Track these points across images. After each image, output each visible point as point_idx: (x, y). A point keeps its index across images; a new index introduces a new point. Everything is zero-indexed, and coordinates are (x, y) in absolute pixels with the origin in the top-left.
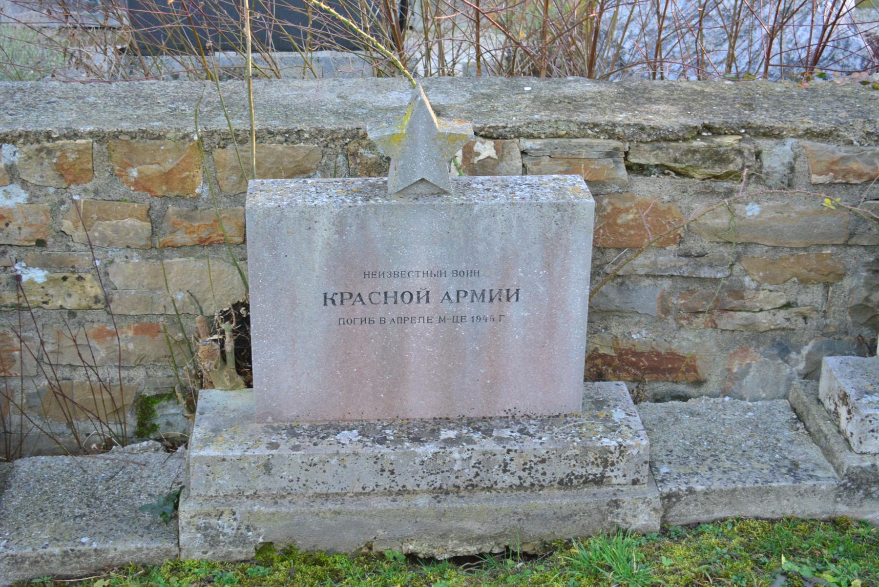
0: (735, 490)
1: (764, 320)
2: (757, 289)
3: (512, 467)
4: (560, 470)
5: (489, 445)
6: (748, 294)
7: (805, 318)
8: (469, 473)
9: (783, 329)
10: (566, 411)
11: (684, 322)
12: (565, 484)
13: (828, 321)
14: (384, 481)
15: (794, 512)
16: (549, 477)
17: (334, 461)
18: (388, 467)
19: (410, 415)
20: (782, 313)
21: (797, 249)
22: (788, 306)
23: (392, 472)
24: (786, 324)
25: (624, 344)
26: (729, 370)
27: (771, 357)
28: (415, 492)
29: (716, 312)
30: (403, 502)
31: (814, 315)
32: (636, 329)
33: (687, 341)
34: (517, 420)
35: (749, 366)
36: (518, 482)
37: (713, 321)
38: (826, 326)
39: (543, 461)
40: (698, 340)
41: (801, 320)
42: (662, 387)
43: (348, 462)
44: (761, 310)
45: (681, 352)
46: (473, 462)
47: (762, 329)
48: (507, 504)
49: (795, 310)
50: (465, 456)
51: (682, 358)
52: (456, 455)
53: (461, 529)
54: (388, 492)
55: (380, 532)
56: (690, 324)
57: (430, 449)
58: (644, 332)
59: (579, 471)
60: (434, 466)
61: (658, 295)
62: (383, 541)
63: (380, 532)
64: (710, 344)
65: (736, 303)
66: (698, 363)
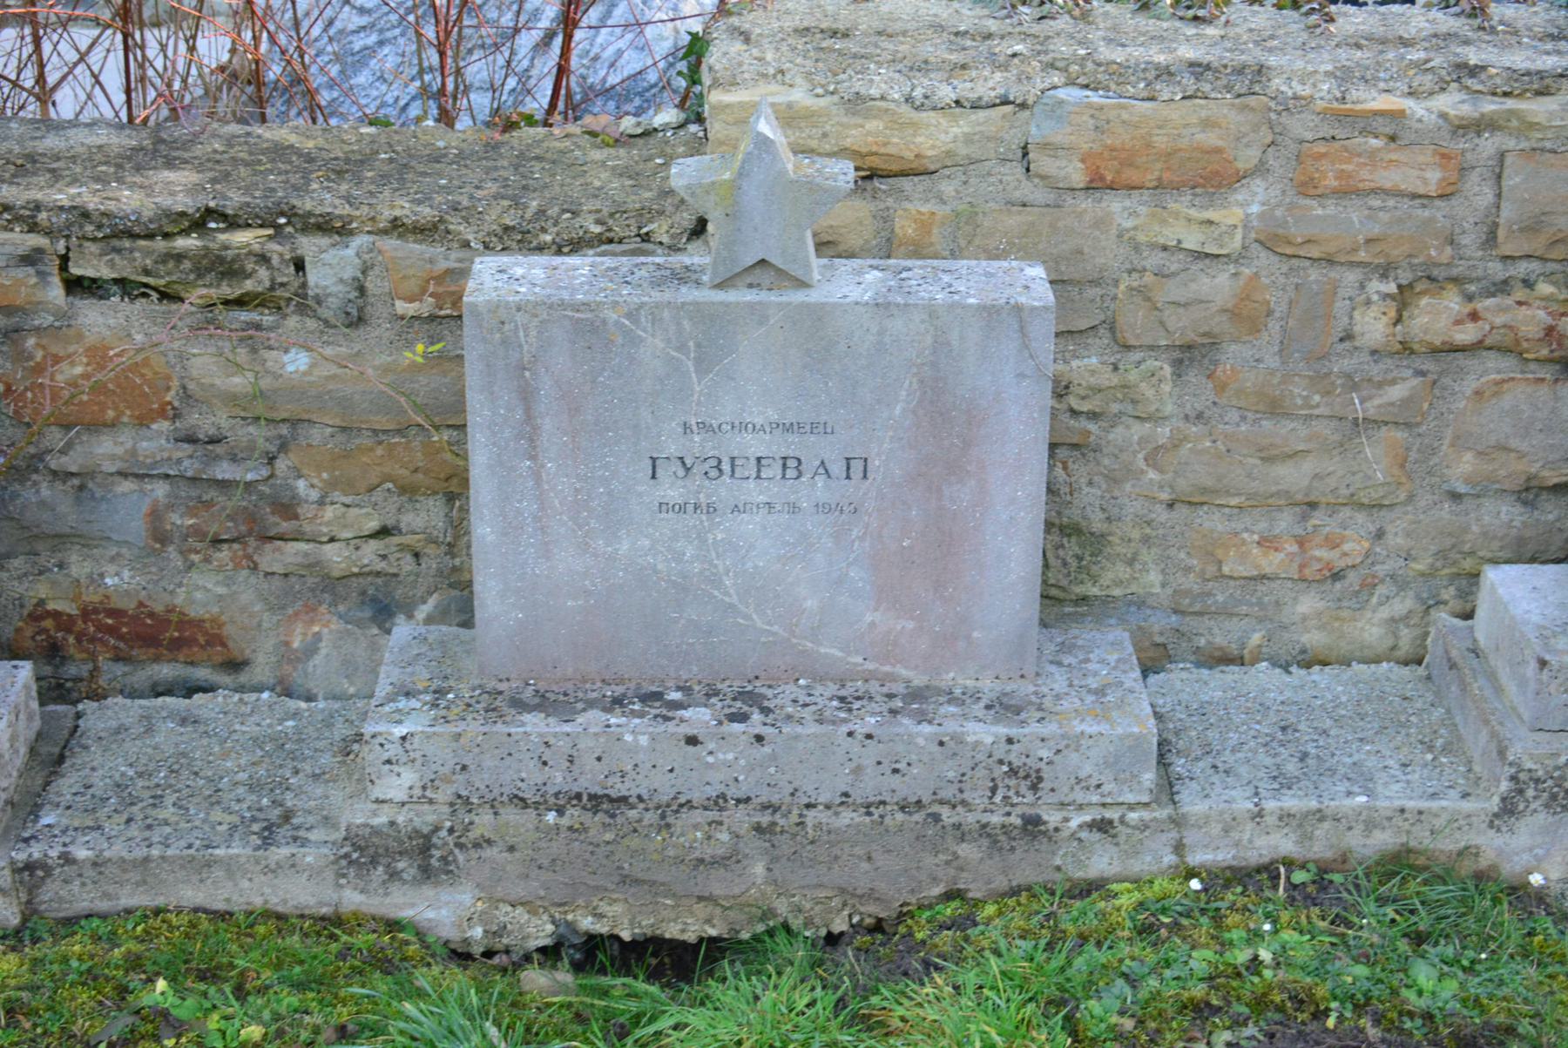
0: (147, 859)
1: (336, 557)
2: (321, 503)
6: (305, 511)
7: (417, 555)
9: (378, 574)
11: (195, 558)
13: (457, 561)
15: (266, 902)
20: (374, 545)
21: (385, 432)
22: (383, 532)
24: (381, 566)
25: (92, 597)
26: (287, 644)
27: (359, 624)
29: (252, 542)
31: (431, 550)
32: (112, 568)
33: (203, 590)
35: (318, 637)
37: (249, 557)
40: (221, 590)
41: (409, 558)
42: (166, 671)
44: (332, 540)
45: (194, 612)
47: (336, 574)
49: (396, 540)
51: (198, 624)
56: (207, 560)
58: (126, 574)
61: (145, 507)
64: (247, 597)
65: (285, 526)
66: (229, 630)
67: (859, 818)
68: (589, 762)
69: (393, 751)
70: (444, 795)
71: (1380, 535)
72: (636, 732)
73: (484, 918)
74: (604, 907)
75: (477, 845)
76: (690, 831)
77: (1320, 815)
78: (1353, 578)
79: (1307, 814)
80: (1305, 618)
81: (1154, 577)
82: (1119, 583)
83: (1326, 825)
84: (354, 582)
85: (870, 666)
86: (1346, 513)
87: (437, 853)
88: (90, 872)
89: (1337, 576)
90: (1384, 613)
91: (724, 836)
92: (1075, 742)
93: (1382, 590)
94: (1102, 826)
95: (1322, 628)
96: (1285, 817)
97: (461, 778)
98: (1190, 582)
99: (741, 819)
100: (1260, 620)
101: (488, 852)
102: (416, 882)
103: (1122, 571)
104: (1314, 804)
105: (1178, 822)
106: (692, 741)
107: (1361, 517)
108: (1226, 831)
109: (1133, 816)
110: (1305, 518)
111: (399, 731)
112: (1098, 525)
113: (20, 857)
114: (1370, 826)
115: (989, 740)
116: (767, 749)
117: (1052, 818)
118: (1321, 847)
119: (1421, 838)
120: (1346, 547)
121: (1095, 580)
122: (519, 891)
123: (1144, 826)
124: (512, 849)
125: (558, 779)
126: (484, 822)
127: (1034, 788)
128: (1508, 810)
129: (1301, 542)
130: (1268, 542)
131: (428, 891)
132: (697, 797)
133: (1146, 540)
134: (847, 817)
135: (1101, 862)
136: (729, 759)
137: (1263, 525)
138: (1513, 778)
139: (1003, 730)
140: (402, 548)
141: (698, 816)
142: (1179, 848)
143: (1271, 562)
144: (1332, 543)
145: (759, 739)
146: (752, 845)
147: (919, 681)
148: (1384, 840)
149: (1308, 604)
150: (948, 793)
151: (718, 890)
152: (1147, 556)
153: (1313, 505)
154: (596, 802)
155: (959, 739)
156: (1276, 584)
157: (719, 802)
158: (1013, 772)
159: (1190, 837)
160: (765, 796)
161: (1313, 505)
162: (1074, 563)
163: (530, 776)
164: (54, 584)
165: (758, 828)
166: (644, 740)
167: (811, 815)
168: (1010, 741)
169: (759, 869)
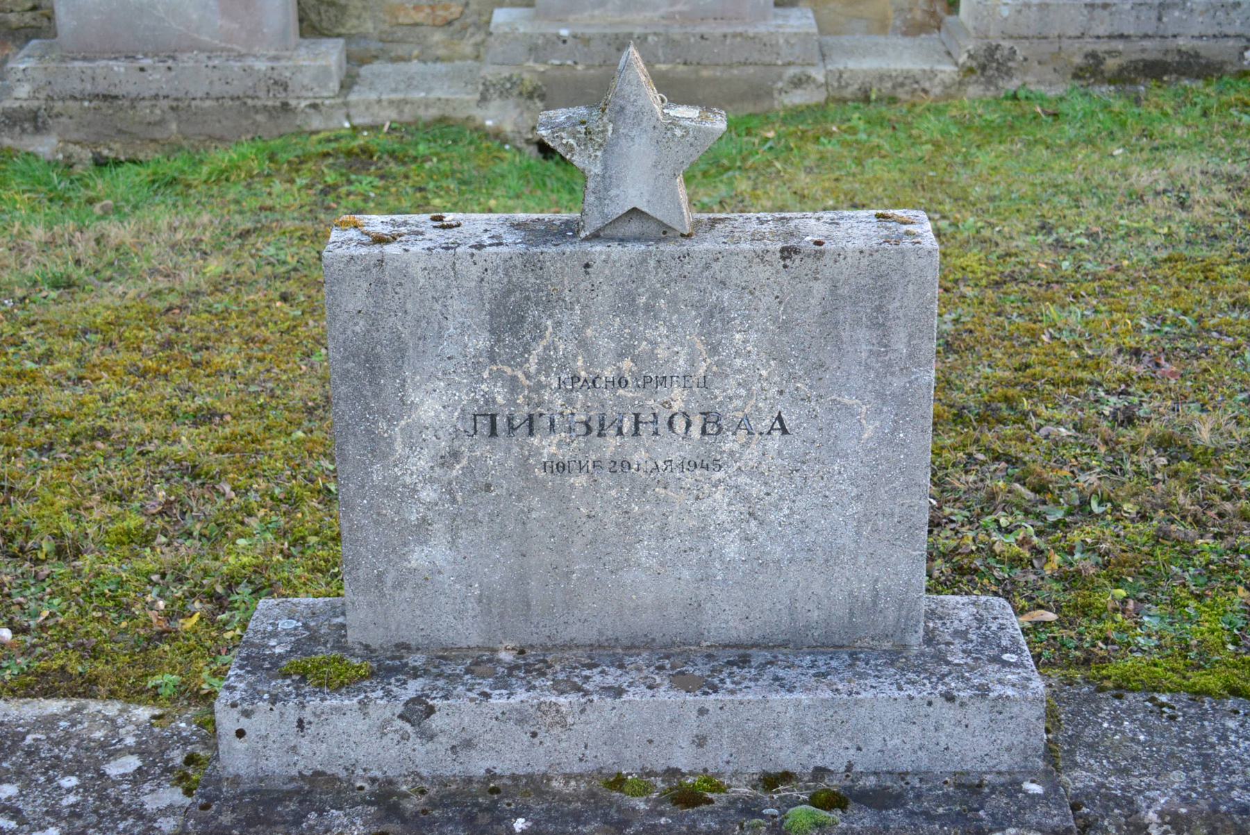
9: (32, 27)
20: (29, 14)
22: (34, 8)
24: (33, 23)
41: (45, 20)
44: (12, 11)
47: (14, 26)
49: (40, 12)
67: (214, 103)
68: (100, 80)
69: (20, 75)
70: (42, 95)
72: (119, 67)
73: (63, 150)
74: (112, 145)
75: (57, 116)
76: (144, 110)
77: (406, 102)
78: (457, 25)
79: (400, 101)
80: (437, 43)
82: (354, 27)
84: (22, 31)
85: (223, 45)
87: (40, 120)
89: (450, 23)
90: (473, 41)
91: (158, 112)
92: (298, 69)
93: (471, 30)
94: (314, 106)
95: (445, 47)
96: (391, 102)
97: (48, 88)
98: (386, 27)
99: (165, 104)
100: (418, 44)
101: (63, 119)
103: (354, 22)
105: (346, 104)
106: (142, 69)
108: (367, 109)
109: (327, 102)
111: (22, 67)
114: (427, 106)
115: (264, 68)
116: (173, 73)
117: (293, 103)
118: (407, 116)
119: (449, 112)
120: (453, 10)
121: (343, 25)
123: (332, 107)
124: (71, 117)
125: (89, 87)
126: (58, 106)
127: (285, 90)
128: (484, 99)
131: (38, 138)
132: (147, 95)
133: (364, 8)
134: (208, 103)
135: (316, 122)
136: (158, 78)
139: (270, 64)
140: (43, 15)
141: (147, 103)
143: (419, 17)
145: (169, 68)
146: (170, 115)
147: (244, 51)
148: (433, 113)
149: (438, 36)
150: (250, 93)
151: (158, 136)
152: (365, 15)
154: (106, 97)
155: (251, 68)
156: (423, 28)
157: (156, 97)
158: (276, 83)
159: (353, 112)
160: (174, 94)
162: (333, 19)
163: (76, 86)
165: (172, 108)
166: (122, 70)
167: (193, 103)
168: (273, 69)
169: (174, 126)
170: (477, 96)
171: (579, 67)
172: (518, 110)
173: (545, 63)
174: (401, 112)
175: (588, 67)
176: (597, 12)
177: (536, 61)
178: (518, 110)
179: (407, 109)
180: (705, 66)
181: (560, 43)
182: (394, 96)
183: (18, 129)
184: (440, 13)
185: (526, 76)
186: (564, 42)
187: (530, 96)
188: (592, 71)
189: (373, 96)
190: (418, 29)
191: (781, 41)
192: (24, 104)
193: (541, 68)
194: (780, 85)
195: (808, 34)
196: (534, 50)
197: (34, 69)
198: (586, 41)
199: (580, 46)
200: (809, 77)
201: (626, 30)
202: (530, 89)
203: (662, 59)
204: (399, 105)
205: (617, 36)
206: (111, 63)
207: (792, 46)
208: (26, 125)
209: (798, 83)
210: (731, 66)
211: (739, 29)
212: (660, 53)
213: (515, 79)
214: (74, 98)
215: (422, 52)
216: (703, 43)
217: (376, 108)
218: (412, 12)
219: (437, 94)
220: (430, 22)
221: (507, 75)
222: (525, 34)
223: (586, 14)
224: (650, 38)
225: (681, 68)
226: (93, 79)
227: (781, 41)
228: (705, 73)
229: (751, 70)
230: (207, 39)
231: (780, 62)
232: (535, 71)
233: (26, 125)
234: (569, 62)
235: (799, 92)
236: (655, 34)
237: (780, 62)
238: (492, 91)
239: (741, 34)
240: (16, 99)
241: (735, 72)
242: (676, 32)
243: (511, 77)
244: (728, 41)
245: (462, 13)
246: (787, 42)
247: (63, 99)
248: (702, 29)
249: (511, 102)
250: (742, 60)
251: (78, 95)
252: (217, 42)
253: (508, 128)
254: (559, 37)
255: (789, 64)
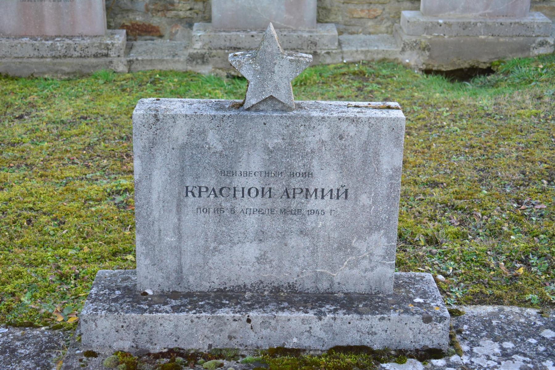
1: (182, 14)
2: (179, 3)
3: (77, 49)
4: (93, 51)
5: (70, 42)
6: (176, 5)
7: (197, 14)
8: (63, 51)
9: (190, 18)
10: (99, 34)
11: (154, 14)
12: (95, 56)
13: (205, 15)
14: (36, 53)
16: (90, 54)
17: (19, 45)
18: (37, 48)
19: (47, 34)
20: (189, 12)
22: (191, 9)
23: (38, 50)
24: (190, 16)
25: (133, 22)
26: (171, 32)
27: (186, 28)
28: (46, 58)
29: (165, 11)
30: (42, 60)
31: (200, 13)
32: (137, 17)
33: (156, 21)
34: (82, 36)
35: (178, 30)
36: (80, 55)
38: (205, 17)
39: (87, 48)
40: (159, 21)
42: (148, 37)
43: (24, 46)
44: (181, 10)
45: (154, 25)
46: (64, 47)
47: (182, 17)
48: (75, 61)
50: (62, 45)
51: (154, 27)
52: (58, 44)
53: (62, 70)
54: (38, 57)
55: (35, 70)
56: (156, 15)
57: (50, 42)
58: (141, 18)
59: (100, 51)
60: (52, 48)
61: (145, 4)
62: (37, 73)
63: (35, 70)
64: (164, 22)
65: (172, 8)
66: (161, 29)
69: (198, 38)
70: (206, 47)
71: (384, 9)
72: (242, 35)
73: (214, 72)
75: (213, 57)
77: (368, 51)
78: (379, 18)
80: (370, 26)
81: (340, 18)
82: (333, 19)
83: (369, 53)
84: (185, 19)
85: (285, 26)
86: (377, 5)
87: (205, 58)
88: (141, 62)
89: (376, 17)
90: (385, 25)
92: (323, 36)
93: (385, 21)
94: (328, 53)
96: (362, 52)
97: (210, 44)
98: (347, 19)
100: (361, 26)
101: (215, 58)
102: (201, 64)
103: (334, 16)
104: (367, 49)
105: (342, 52)
106: (253, 36)
107: (380, 6)
108: (351, 54)
109: (334, 51)
110: (369, 6)
112: (329, 7)
113: (128, 59)
114: (378, 53)
115: (307, 36)
117: (319, 51)
119: (387, 56)
121: (329, 18)
122: (220, 66)
123: (336, 53)
124: (219, 57)
125: (228, 44)
126: (214, 52)
127: (315, 46)
128: (403, 50)
129: (369, 10)
130: (362, 11)
131: (204, 66)
132: (253, 47)
133: (339, 10)
135: (328, 60)
137: (361, 7)
138: (404, 44)
139: (310, 34)
140: (195, 12)
142: (343, 58)
143: (363, 15)
144: (375, 11)
147: (294, 28)
148: (380, 56)
149: (370, 23)
150: (300, 47)
153: (371, 3)
155: (301, 36)
158: (312, 43)
159: (345, 56)
161: (371, 3)
163: (222, 43)
164: (126, 20)
166: (244, 36)
168: (311, 36)
170: (400, 49)
171: (446, 37)
172: (418, 56)
173: (431, 35)
174: (366, 56)
175: (450, 37)
176: (451, 13)
177: (427, 34)
178: (418, 56)
179: (369, 54)
180: (502, 37)
181: (439, 26)
182: (363, 49)
183: (195, 62)
184: (373, 13)
185: (423, 40)
186: (441, 25)
187: (424, 49)
188: (452, 39)
189: (354, 49)
190: (362, 20)
191: (535, 26)
192: (199, 51)
193: (429, 37)
194: (534, 45)
195: (547, 23)
196: (427, 29)
197: (204, 36)
198: (450, 25)
199: (447, 28)
200: (547, 42)
201: (468, 21)
202: (424, 46)
203: (483, 33)
204: (365, 53)
205: (464, 23)
206: (238, 33)
207: (540, 28)
208: (199, 61)
209: (542, 44)
210: (512, 37)
211: (517, 21)
212: (482, 31)
213: (418, 42)
214: (221, 49)
215: (363, 30)
216: (501, 26)
217: (355, 55)
218: (360, 12)
219: (382, 48)
220: (367, 17)
221: (414, 40)
222: (423, 22)
223: (447, 14)
224: (478, 24)
225: (491, 37)
226: (230, 40)
227: (535, 26)
228: (501, 40)
229: (522, 39)
230: (279, 23)
231: (534, 35)
232: (426, 38)
233: (199, 61)
234: (442, 35)
235: (542, 48)
236: (481, 22)
237: (534, 35)
238: (407, 47)
239: (518, 23)
240: (195, 49)
241: (515, 39)
242: (489, 21)
243: (416, 41)
244: (512, 26)
245: (382, 13)
246: (538, 26)
247: (216, 49)
248: (501, 20)
249: (415, 52)
250: (518, 34)
251: (223, 48)
252: (283, 24)
253: (412, 63)
254: (438, 23)
255: (538, 36)
